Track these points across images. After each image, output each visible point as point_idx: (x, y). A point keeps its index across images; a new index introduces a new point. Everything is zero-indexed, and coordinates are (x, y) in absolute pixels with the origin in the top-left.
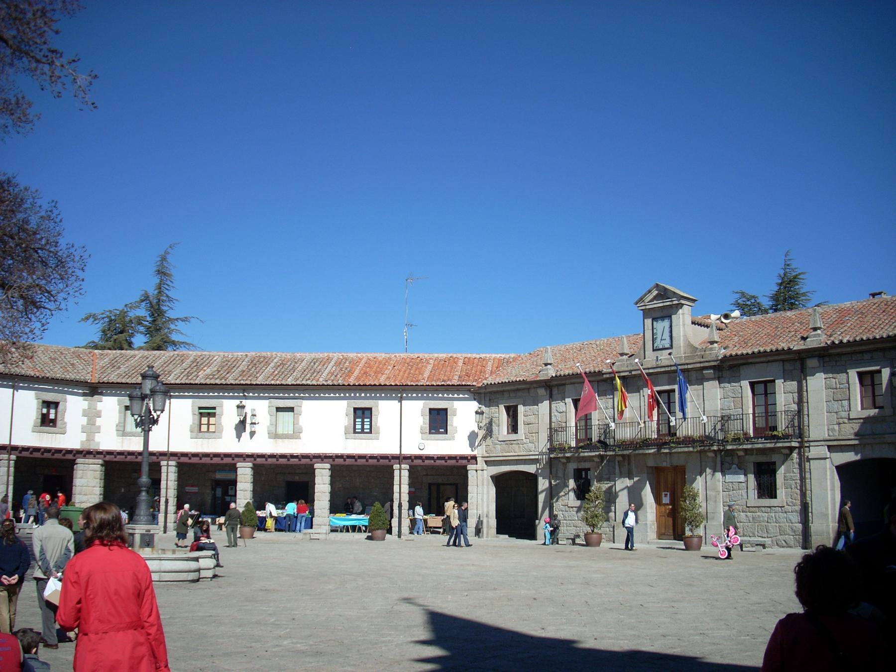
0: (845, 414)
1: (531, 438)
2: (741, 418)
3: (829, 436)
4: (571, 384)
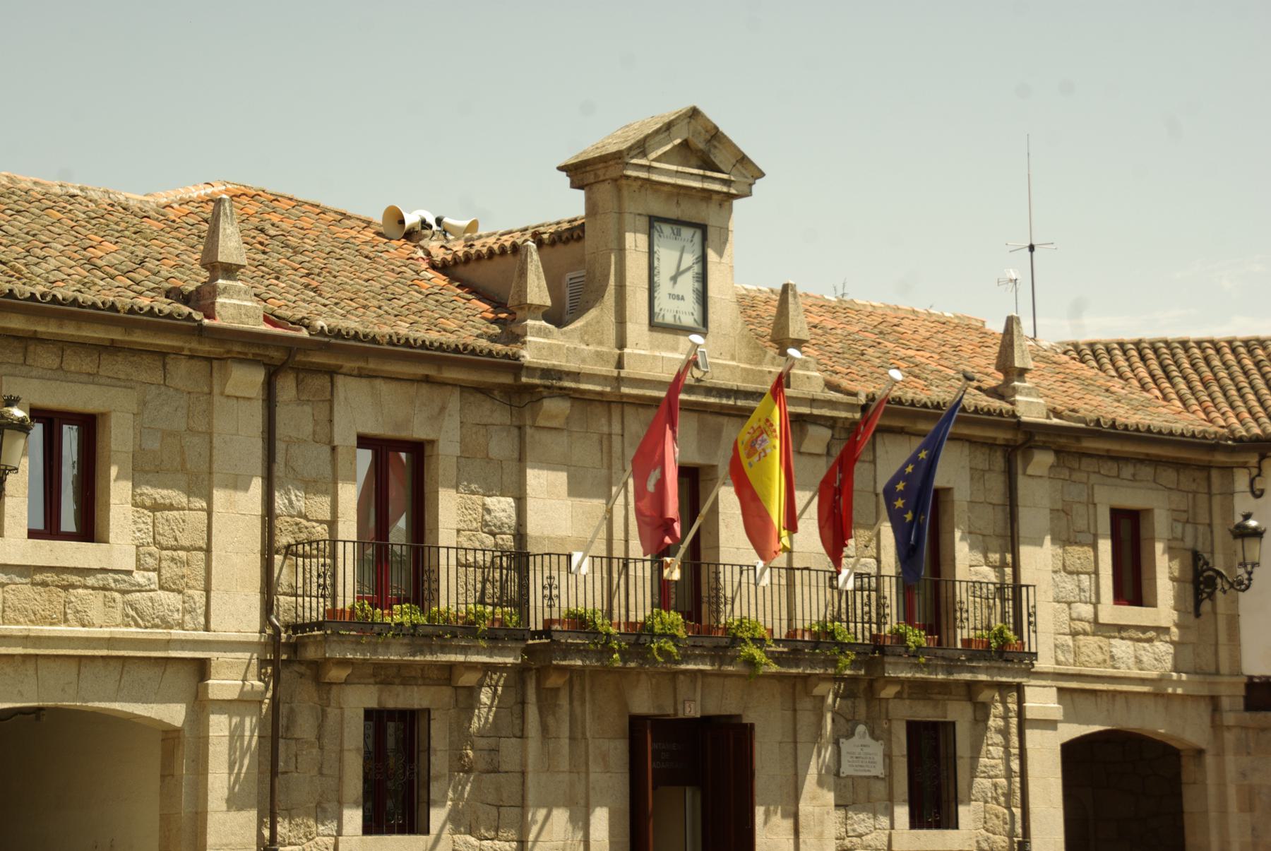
0: (1086, 610)
1: (169, 570)
2: (873, 585)
3: (1058, 663)
4: (361, 374)
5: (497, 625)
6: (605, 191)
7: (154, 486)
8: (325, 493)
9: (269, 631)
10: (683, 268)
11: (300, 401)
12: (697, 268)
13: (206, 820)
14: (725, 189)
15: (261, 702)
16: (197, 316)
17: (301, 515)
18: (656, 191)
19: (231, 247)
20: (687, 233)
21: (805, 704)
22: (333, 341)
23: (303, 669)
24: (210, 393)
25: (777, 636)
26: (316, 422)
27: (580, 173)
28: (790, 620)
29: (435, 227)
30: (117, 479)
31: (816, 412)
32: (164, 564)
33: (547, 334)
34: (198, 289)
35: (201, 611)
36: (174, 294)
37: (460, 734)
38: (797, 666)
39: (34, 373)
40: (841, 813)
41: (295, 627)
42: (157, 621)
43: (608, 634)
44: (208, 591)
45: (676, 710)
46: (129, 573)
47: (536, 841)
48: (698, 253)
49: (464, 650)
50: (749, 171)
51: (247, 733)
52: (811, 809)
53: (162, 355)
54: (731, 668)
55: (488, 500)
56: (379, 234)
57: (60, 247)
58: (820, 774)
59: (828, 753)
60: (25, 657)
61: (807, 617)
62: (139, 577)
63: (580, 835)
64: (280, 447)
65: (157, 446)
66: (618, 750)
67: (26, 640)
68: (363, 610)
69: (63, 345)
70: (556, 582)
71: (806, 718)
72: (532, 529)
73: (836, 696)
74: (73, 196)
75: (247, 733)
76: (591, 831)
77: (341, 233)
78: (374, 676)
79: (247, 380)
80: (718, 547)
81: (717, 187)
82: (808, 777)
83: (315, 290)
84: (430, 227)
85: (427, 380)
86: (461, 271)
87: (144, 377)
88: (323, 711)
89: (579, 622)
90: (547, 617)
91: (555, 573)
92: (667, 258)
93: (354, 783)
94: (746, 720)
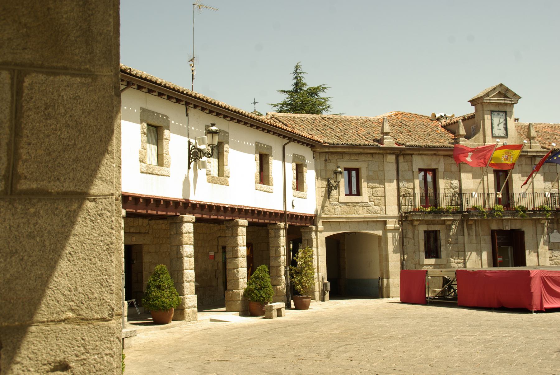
2: (558, 196)
4: (419, 155)
5: (454, 210)
6: (479, 106)
7: (372, 183)
8: (412, 182)
9: (400, 214)
10: (500, 122)
11: (405, 162)
12: (504, 122)
13: (388, 256)
14: (511, 102)
15: (399, 230)
16: (379, 145)
17: (406, 187)
18: (492, 104)
19: (387, 128)
20: (501, 114)
21: (539, 226)
22: (411, 148)
23: (408, 222)
24: (383, 162)
25: (529, 209)
26: (408, 166)
27: (473, 102)
28: (534, 205)
29: (444, 117)
30: (363, 182)
31: (538, 154)
32: (375, 200)
33: (465, 141)
34: (380, 139)
35: (384, 210)
36: (375, 140)
37: (448, 236)
38: (535, 217)
39: (344, 160)
40: (551, 251)
41: (405, 213)
42: (374, 213)
43: (483, 211)
44: (385, 206)
45: (503, 228)
46: (367, 202)
47: (468, 259)
48: (504, 118)
49: (446, 216)
50: (517, 97)
51: (396, 237)
52: (542, 251)
53: (372, 154)
54: (517, 218)
55: (452, 181)
56: (430, 120)
57: (352, 132)
58: (544, 242)
59: (546, 237)
60: (346, 221)
61: (537, 204)
62: (370, 203)
63: (479, 258)
64: (400, 172)
65: (372, 174)
66: (489, 238)
67: (346, 218)
68: (421, 208)
69: (350, 154)
70: (469, 200)
71: (539, 229)
72: (463, 187)
73: (548, 223)
74: (358, 119)
75: (396, 237)
76: (482, 257)
77: (420, 120)
78: (426, 223)
79: (391, 158)
80: (513, 189)
81: (508, 102)
82: (541, 243)
83: (410, 136)
84: (443, 117)
85: (435, 154)
86: (448, 127)
87: (368, 159)
88: (414, 231)
89: (476, 209)
90: (467, 208)
91: (468, 197)
92: (496, 120)
93: (422, 247)
94: (522, 230)
